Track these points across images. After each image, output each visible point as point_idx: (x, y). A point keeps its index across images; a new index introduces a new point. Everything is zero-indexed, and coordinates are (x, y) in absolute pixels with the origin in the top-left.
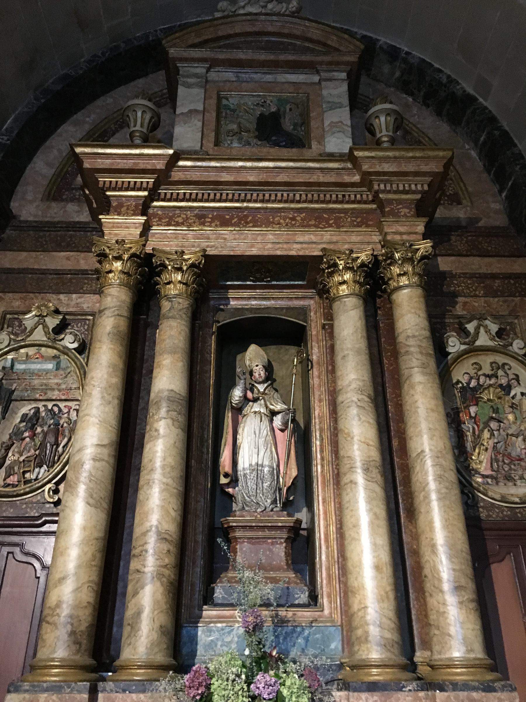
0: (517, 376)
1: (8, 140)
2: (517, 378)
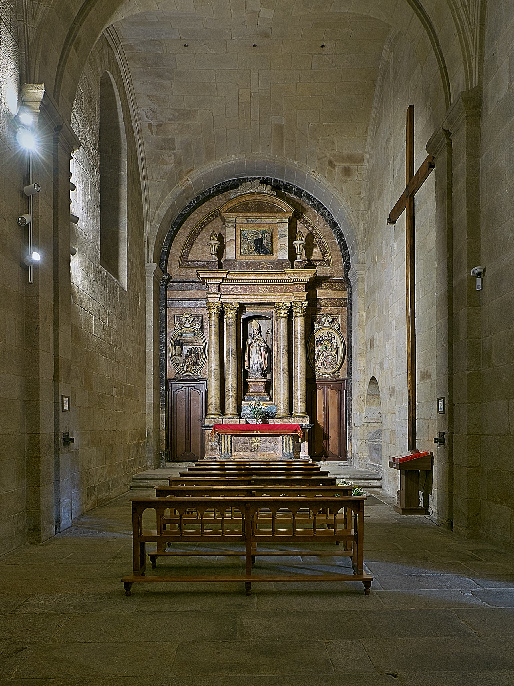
0: (334, 336)
1: (166, 249)
2: (334, 338)
